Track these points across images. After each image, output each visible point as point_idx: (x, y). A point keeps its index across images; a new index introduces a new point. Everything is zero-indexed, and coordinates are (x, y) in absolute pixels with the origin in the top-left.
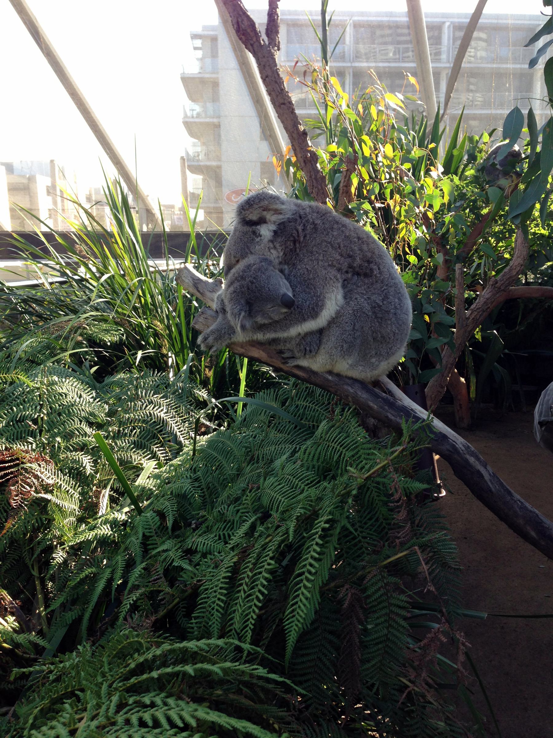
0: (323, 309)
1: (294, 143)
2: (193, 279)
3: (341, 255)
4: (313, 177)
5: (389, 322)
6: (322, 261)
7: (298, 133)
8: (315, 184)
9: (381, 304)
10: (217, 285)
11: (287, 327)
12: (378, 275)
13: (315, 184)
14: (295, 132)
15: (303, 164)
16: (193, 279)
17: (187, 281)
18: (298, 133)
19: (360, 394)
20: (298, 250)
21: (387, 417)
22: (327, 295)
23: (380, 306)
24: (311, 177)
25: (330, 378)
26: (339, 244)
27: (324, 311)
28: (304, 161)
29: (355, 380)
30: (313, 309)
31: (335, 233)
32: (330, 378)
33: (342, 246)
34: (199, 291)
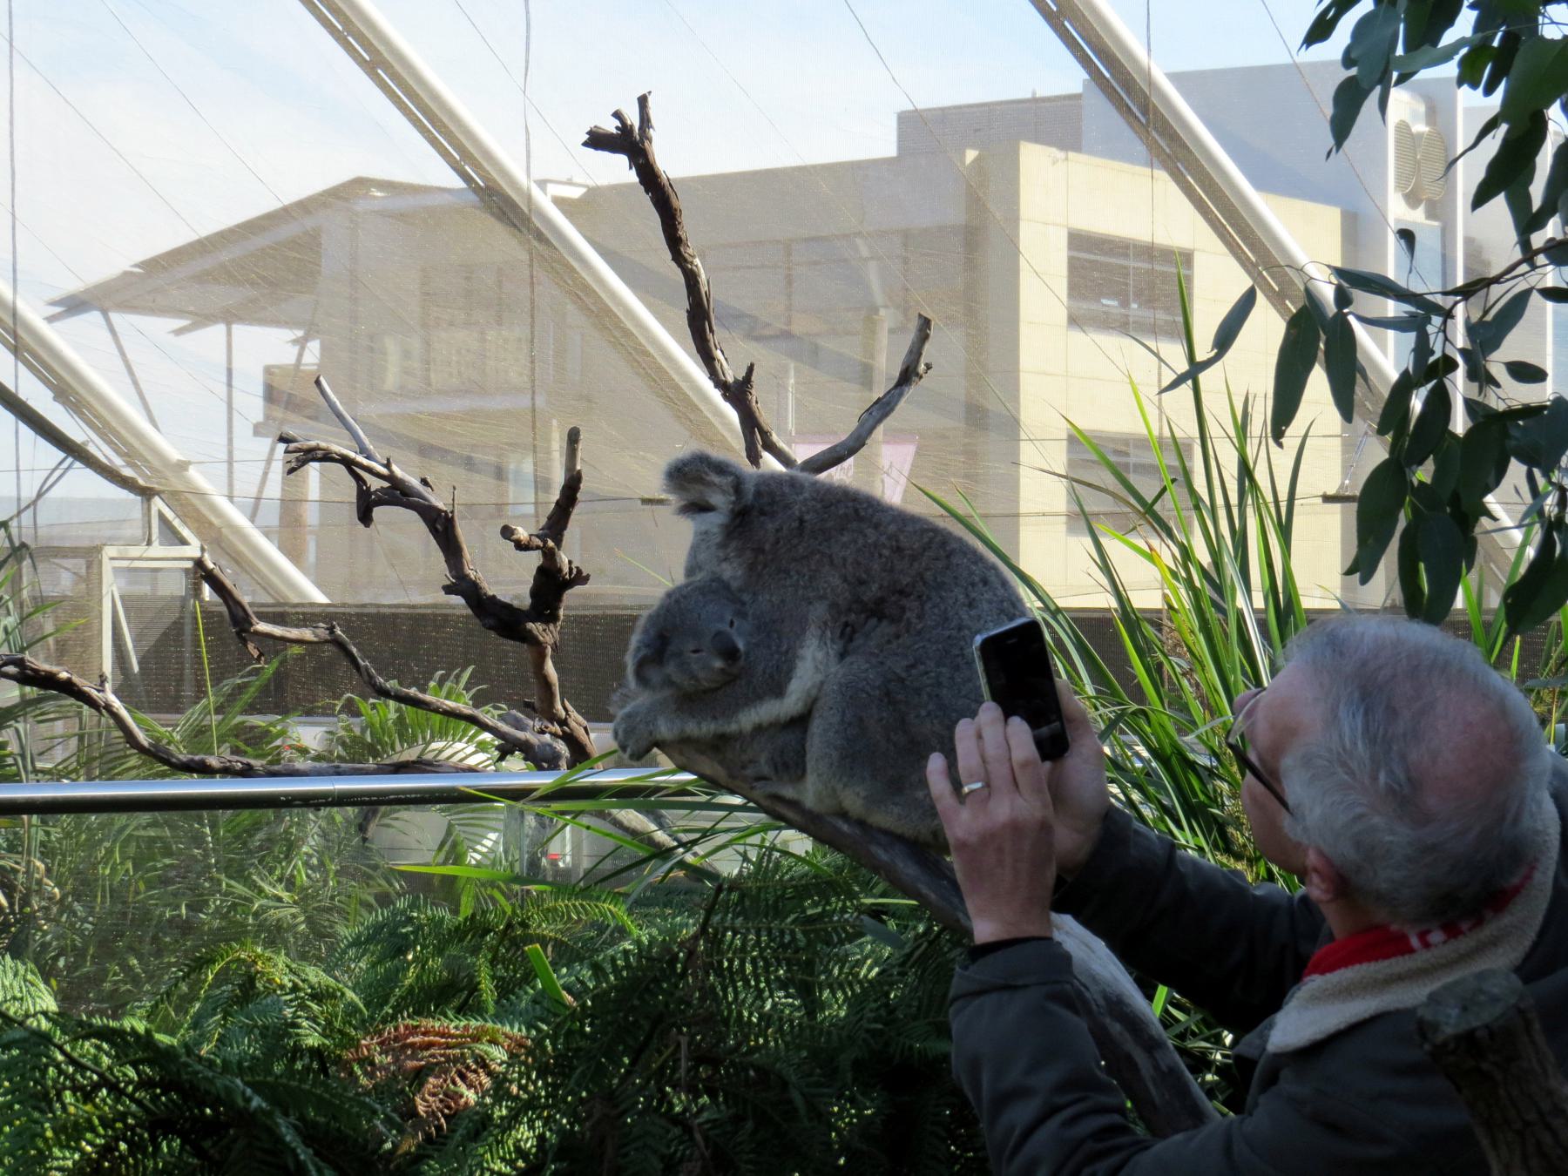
0: (790, 679)
3: (845, 580)
5: (923, 713)
6: (805, 588)
9: (904, 675)
11: (731, 711)
12: (914, 621)
19: (901, 865)
20: (759, 568)
22: (801, 652)
23: (902, 680)
25: (845, 827)
26: (844, 559)
27: (793, 681)
29: (899, 838)
30: (771, 676)
31: (845, 539)
32: (845, 827)
33: (850, 560)
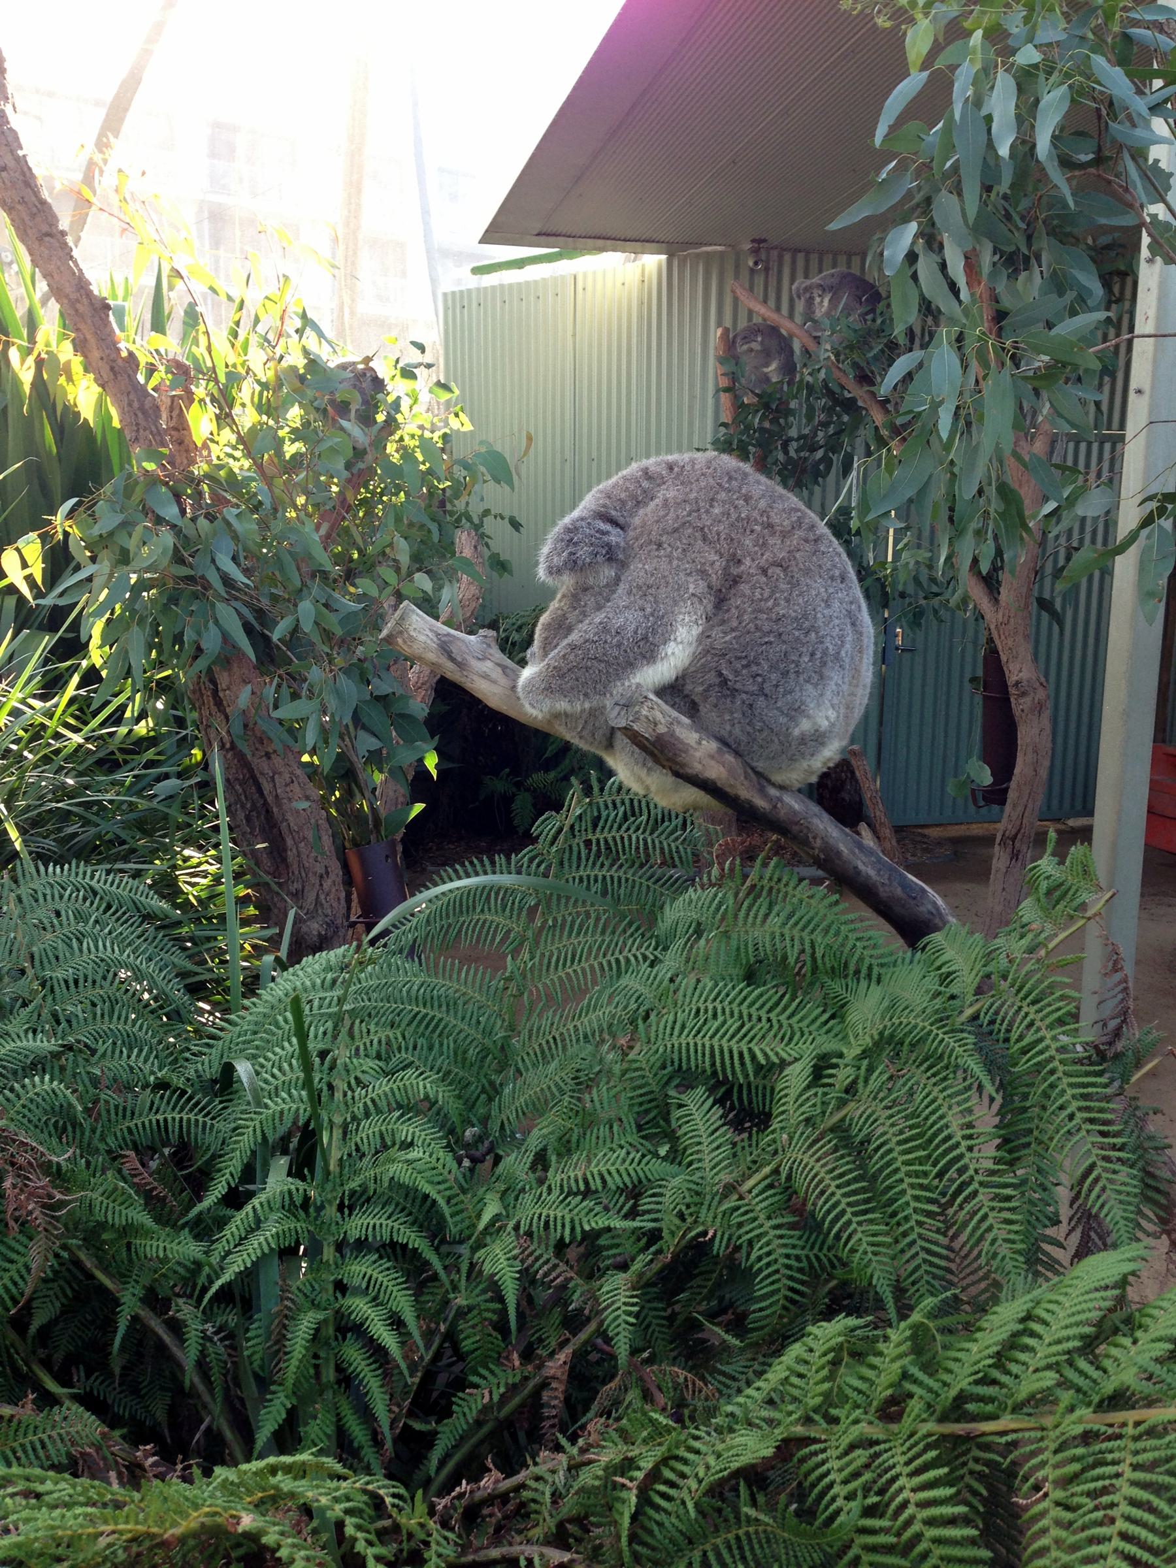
1: (82, 326)
2: (438, 635)
4: (136, 405)
7: (92, 304)
8: (143, 423)
10: (489, 646)
13: (143, 423)
14: (85, 301)
15: (106, 374)
16: (438, 635)
17: (422, 638)
18: (92, 304)
21: (856, 868)
24: (130, 405)
28: (112, 369)
34: (453, 660)
